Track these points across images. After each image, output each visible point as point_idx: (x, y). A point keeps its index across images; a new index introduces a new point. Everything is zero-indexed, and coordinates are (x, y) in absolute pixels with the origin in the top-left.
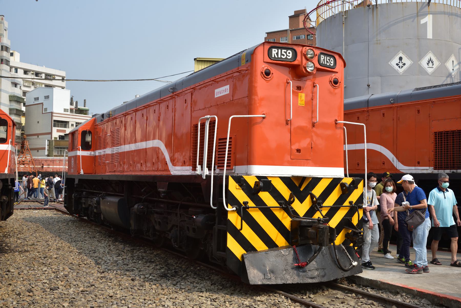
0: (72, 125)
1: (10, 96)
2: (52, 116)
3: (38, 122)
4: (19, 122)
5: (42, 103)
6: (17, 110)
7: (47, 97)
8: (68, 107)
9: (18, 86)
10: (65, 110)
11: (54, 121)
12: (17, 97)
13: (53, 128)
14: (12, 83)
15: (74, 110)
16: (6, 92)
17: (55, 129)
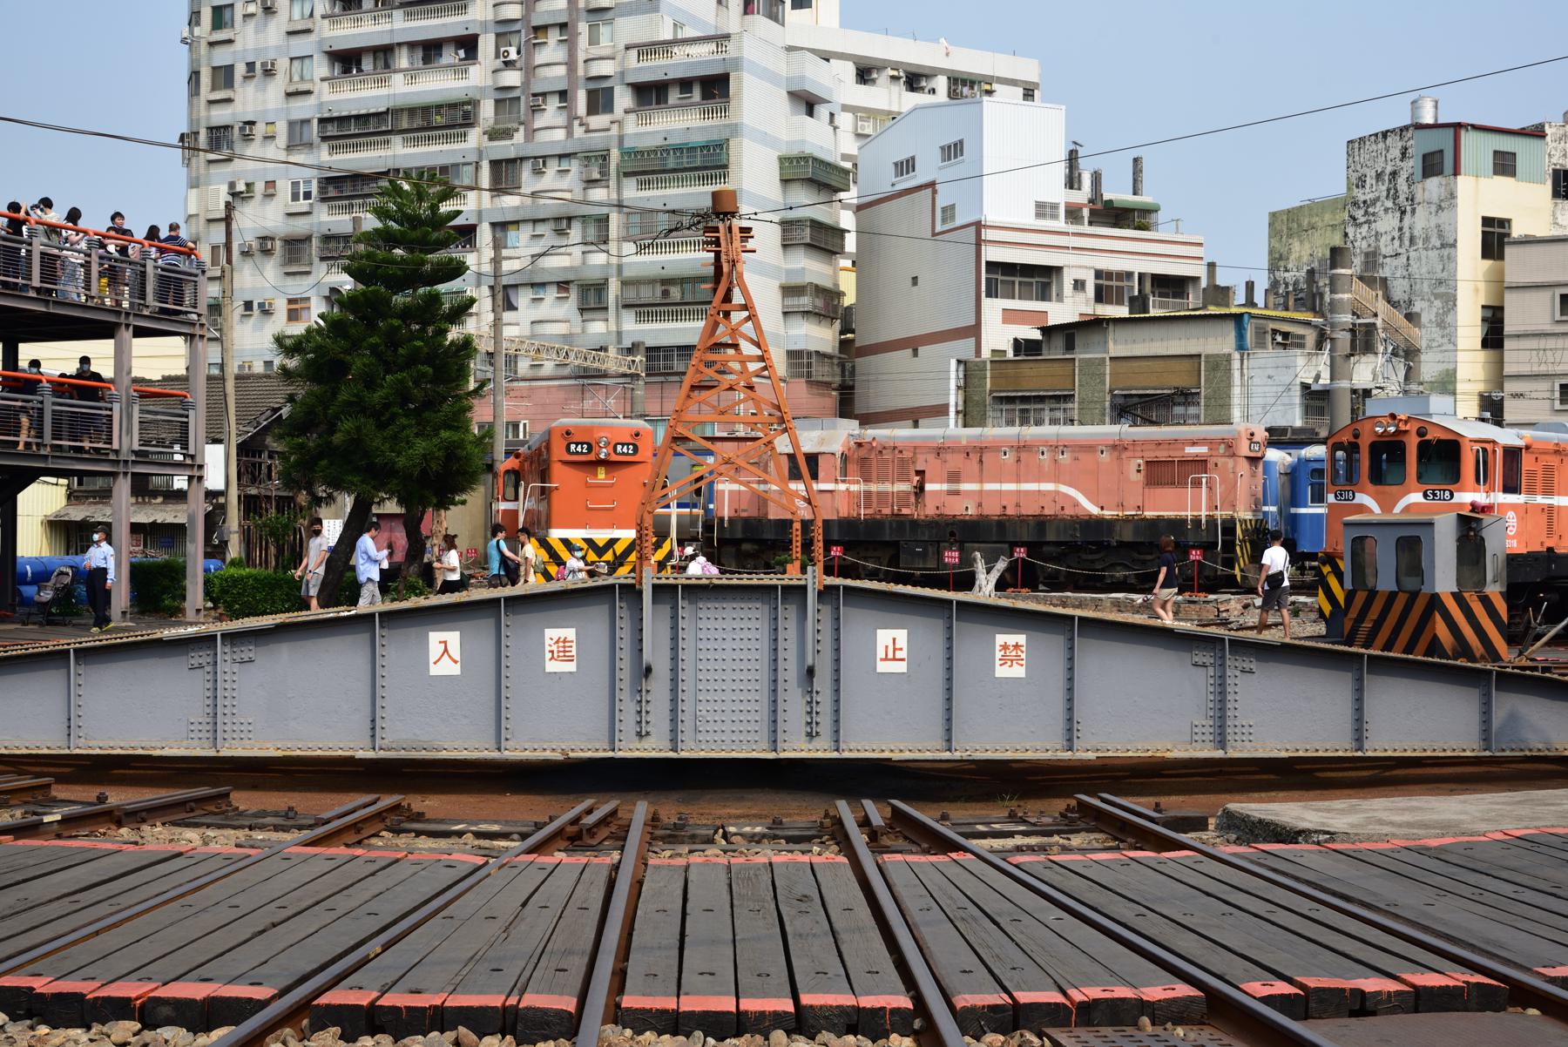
0: (1079, 285)
1: (782, 160)
2: (979, 243)
3: (915, 280)
4: (828, 284)
5: (932, 184)
6: (816, 225)
7: (953, 151)
8: (1060, 195)
9: (822, 111)
10: (1043, 210)
11: (992, 266)
12: (815, 159)
13: (987, 303)
14: (794, 95)
15: (1086, 212)
16: (765, 139)
17: (993, 308)
